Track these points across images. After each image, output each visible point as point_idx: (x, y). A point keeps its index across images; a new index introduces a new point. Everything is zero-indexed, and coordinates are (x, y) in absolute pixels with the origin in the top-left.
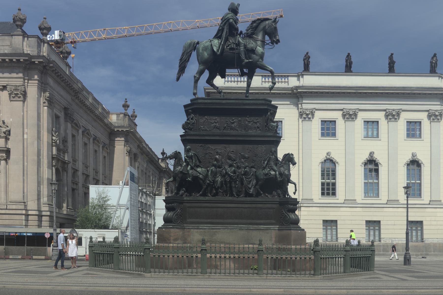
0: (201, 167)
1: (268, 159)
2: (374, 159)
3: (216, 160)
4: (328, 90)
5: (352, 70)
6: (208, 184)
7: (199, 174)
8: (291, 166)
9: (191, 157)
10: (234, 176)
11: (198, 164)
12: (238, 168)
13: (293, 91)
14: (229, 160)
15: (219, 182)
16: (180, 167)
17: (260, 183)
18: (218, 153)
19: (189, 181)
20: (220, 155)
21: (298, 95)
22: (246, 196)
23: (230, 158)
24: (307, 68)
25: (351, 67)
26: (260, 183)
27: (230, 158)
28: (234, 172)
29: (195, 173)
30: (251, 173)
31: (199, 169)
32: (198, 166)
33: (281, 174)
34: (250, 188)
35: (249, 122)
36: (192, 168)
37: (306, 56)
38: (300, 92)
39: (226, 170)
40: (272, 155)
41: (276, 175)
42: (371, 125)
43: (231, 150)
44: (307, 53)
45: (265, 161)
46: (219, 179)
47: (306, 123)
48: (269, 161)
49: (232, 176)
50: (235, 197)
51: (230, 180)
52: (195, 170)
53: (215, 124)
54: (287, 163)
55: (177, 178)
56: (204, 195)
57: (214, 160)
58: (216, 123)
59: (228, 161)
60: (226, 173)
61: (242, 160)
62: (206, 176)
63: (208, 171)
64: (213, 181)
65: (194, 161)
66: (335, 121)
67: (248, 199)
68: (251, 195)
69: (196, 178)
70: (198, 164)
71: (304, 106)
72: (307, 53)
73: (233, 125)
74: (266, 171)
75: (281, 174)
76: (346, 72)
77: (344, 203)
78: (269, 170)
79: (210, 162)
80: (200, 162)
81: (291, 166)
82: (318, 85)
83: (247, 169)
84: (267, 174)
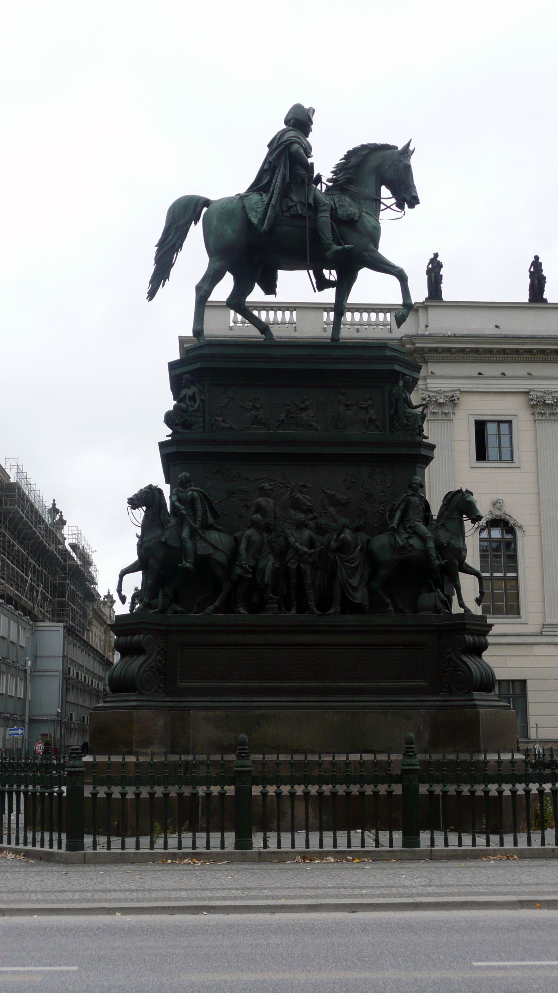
0: (219, 531)
1: (402, 506)
3: (259, 509)
4: (492, 343)
5: (545, 297)
6: (240, 577)
7: (211, 551)
8: (468, 524)
9: (191, 504)
10: (311, 555)
11: (211, 520)
12: (320, 530)
13: (403, 345)
14: (295, 509)
15: (268, 573)
16: (159, 532)
17: (383, 572)
18: (263, 492)
19: (186, 569)
20: (268, 496)
21: (416, 355)
22: (343, 612)
23: (297, 505)
25: (542, 290)
26: (383, 572)
27: (297, 505)
28: (311, 544)
29: (203, 549)
30: (357, 546)
31: (213, 536)
32: (211, 527)
33: (439, 547)
34: (355, 589)
35: (347, 406)
36: (193, 533)
38: (422, 349)
39: (286, 539)
40: (414, 495)
41: (426, 550)
43: (301, 483)
44: (436, 255)
45: (393, 511)
46: (269, 563)
48: (405, 513)
49: (305, 553)
50: (313, 613)
51: (299, 567)
52: (202, 538)
53: (254, 412)
54: (456, 515)
55: (151, 561)
56: (228, 607)
57: (252, 509)
58: (257, 409)
59: (292, 512)
60: (288, 545)
61: (331, 509)
62: (234, 554)
63: (237, 541)
64: (254, 568)
65: (199, 513)
66: (510, 422)
67: (351, 618)
68: (357, 609)
69: (203, 562)
70: (211, 520)
72: (436, 255)
73: (303, 415)
75: (439, 547)
78: (406, 535)
79: (241, 516)
80: (215, 515)
81: (468, 524)
82: (465, 332)
83: (347, 535)
84: (403, 548)
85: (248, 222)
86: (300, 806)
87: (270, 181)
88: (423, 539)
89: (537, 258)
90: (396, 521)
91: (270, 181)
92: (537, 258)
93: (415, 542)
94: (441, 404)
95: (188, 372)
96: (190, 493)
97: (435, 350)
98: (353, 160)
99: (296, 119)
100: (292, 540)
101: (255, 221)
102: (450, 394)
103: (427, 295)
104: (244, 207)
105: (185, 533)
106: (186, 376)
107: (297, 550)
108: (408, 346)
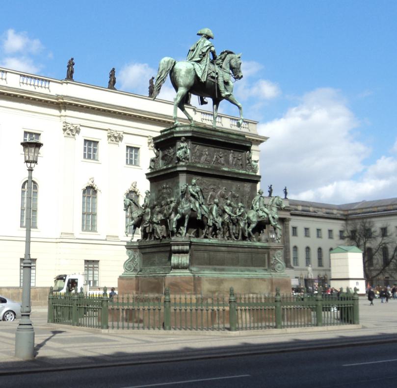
2: (136, 190)
7: (205, 213)
21: (61, 105)
23: (223, 196)
24: (70, 76)
36: (200, 205)
37: (70, 62)
41: (269, 218)
42: (91, 146)
44: (72, 59)
47: (70, 140)
50: (234, 240)
71: (68, 120)
72: (72, 59)
74: (261, 213)
76: (109, 88)
77: (106, 240)
85: (196, 76)
86: (244, 313)
87: (201, 60)
88: (267, 214)
89: (114, 69)
90: (258, 206)
91: (201, 60)
92: (114, 69)
93: (264, 214)
94: (71, 130)
95: (184, 137)
96: (197, 189)
97: (71, 104)
98: (223, 56)
99: (207, 35)
100: (227, 210)
101: (199, 75)
102: (75, 126)
103: (66, 77)
104: (194, 69)
105: (197, 205)
106: (184, 138)
107: (230, 215)
108: (60, 100)
